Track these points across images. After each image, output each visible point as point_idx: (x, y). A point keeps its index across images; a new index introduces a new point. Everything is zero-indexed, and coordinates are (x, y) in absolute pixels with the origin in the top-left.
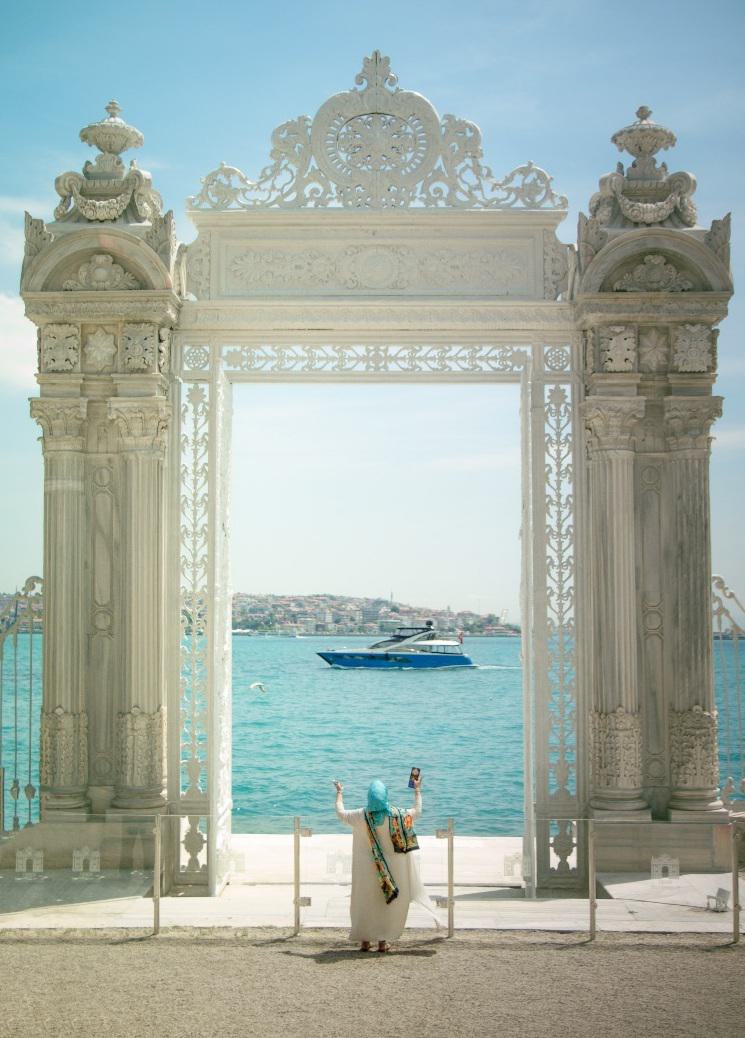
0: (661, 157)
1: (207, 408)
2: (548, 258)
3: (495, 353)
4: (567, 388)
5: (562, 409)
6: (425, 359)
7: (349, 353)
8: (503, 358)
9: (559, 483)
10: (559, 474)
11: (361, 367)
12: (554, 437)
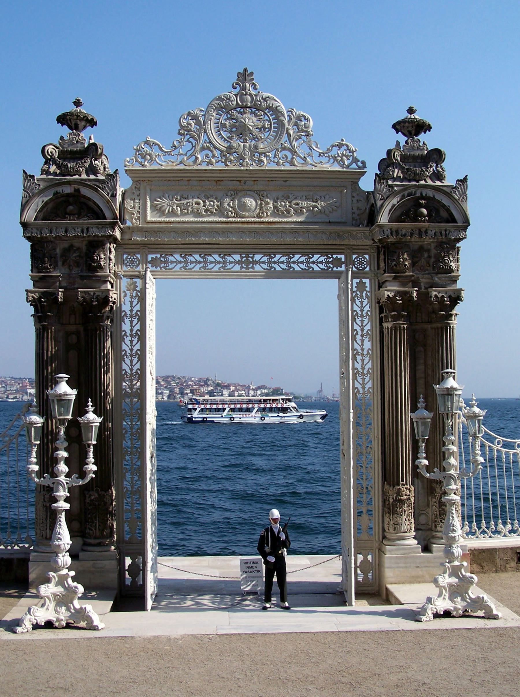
0: (422, 137)
1: (139, 294)
2: (355, 200)
3: (322, 259)
4: (367, 281)
5: (364, 294)
6: (278, 263)
7: (229, 259)
8: (327, 263)
9: (362, 341)
10: (362, 336)
11: (237, 267)
12: (360, 313)
